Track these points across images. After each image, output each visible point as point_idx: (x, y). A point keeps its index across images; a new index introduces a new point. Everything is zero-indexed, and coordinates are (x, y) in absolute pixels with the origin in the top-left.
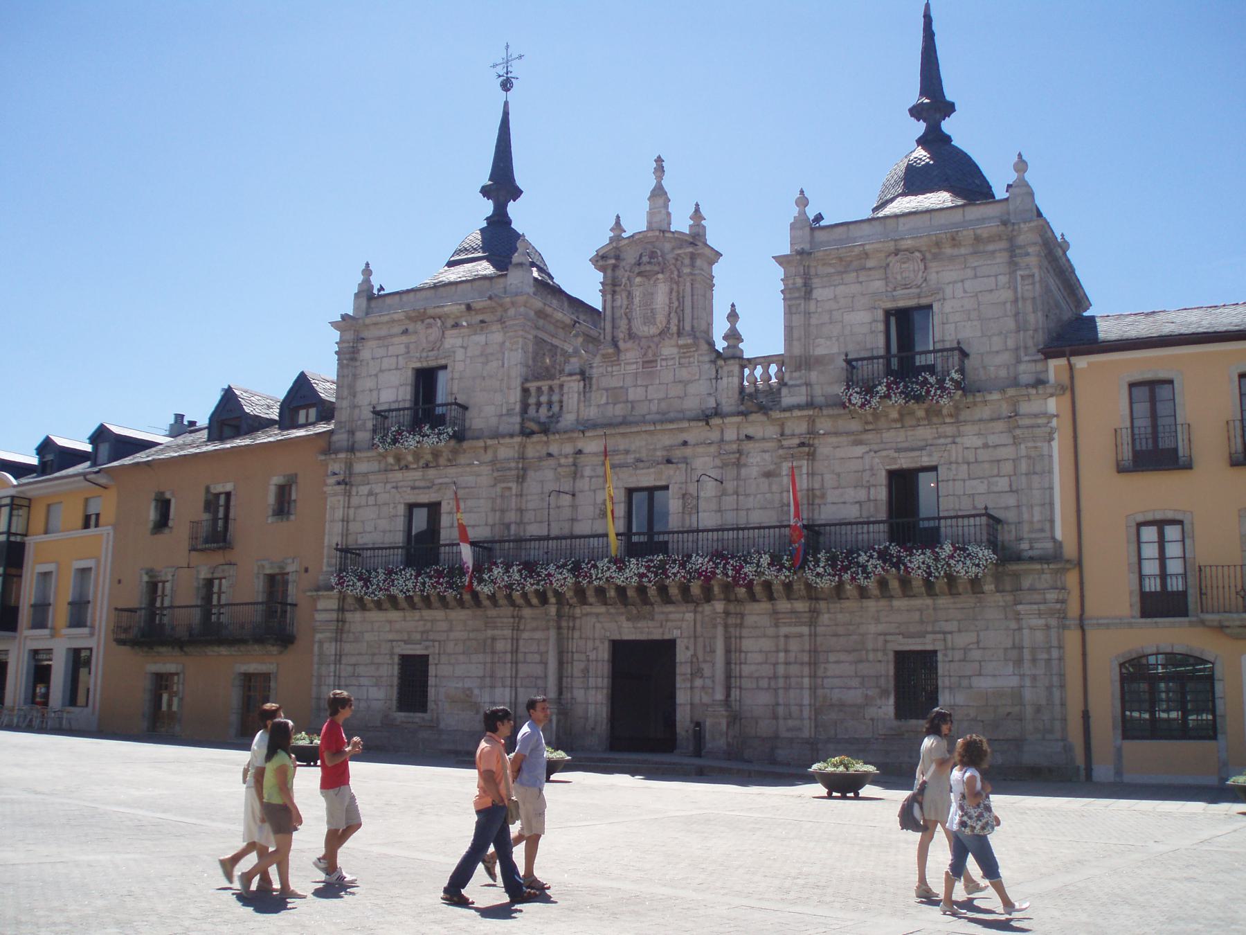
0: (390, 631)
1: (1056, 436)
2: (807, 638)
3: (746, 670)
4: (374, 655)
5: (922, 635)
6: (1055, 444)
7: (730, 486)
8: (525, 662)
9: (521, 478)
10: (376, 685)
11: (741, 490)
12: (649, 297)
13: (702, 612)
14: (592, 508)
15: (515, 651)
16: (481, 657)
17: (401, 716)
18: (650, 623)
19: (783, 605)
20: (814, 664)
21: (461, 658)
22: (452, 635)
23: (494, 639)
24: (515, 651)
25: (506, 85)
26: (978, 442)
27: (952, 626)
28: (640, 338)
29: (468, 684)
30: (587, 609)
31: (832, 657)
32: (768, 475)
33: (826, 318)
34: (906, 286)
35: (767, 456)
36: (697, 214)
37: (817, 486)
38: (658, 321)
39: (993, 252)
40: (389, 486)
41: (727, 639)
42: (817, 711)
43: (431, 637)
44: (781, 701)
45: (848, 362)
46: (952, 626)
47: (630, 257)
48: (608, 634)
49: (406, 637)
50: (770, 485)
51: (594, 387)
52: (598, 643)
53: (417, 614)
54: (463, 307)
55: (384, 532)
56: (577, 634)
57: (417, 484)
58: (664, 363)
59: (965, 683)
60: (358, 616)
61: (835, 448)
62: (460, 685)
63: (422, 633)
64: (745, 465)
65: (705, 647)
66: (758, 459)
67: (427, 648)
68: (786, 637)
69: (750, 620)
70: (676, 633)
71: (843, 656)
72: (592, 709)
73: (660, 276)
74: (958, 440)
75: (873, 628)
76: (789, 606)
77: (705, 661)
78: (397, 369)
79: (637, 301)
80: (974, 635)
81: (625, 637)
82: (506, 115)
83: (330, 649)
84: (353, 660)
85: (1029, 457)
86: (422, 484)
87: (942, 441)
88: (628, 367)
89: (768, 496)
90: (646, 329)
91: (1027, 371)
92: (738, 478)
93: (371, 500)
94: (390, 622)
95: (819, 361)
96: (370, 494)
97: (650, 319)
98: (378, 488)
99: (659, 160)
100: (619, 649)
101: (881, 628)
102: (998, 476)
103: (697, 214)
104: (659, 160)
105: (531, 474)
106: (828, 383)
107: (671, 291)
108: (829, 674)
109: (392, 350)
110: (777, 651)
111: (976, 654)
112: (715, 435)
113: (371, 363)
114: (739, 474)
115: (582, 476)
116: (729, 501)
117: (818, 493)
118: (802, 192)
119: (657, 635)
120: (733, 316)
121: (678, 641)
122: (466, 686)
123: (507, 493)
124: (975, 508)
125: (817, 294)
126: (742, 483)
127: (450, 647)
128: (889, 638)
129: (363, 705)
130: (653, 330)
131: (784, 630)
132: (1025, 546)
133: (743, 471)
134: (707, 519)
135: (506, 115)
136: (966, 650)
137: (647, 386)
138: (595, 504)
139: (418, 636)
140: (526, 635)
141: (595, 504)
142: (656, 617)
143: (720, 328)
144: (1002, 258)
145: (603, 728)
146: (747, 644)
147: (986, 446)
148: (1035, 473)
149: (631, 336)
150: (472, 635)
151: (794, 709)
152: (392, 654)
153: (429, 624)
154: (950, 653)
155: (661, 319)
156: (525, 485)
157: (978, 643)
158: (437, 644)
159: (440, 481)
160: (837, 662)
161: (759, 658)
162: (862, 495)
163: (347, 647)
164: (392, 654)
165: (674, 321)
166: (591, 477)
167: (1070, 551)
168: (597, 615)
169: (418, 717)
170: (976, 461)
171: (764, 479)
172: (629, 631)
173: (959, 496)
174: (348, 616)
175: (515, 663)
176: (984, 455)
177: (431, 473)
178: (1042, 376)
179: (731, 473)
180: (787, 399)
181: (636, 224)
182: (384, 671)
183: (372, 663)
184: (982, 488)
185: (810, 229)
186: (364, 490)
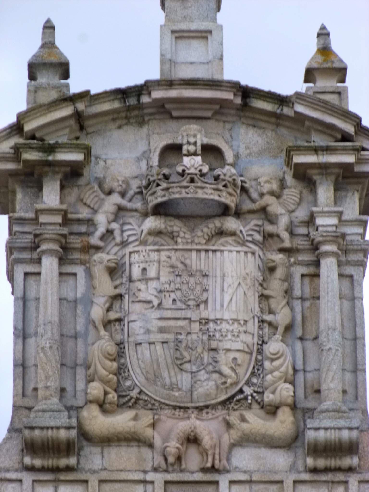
28: (152, 405)
36: (327, 67)
73: (231, 224)
79: (148, 292)
90: (185, 380)
103: (327, 67)
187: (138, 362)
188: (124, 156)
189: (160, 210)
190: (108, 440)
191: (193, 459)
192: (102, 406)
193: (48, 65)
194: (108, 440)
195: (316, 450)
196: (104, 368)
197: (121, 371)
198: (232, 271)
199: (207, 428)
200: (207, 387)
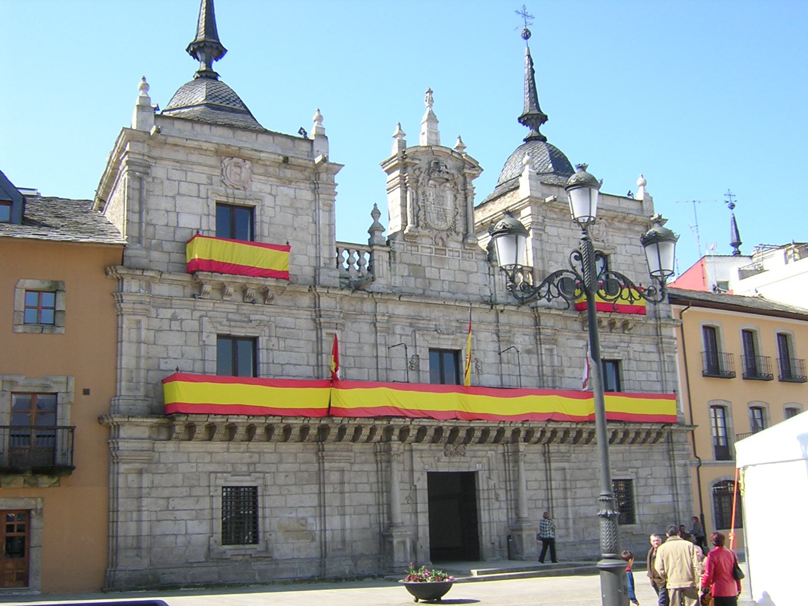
0: (211, 462)
4: (192, 487)
5: (626, 469)
10: (197, 518)
12: (440, 199)
18: (463, 459)
21: (293, 489)
22: (282, 467)
27: (638, 464)
28: (431, 229)
31: (579, 484)
32: (529, 352)
35: (527, 338)
40: (197, 314)
43: (258, 470)
48: (426, 467)
49: (230, 469)
50: (530, 360)
51: (398, 260)
54: (281, 158)
55: (194, 360)
57: (231, 316)
58: (451, 253)
59: (647, 499)
61: (568, 339)
63: (249, 464)
66: (521, 340)
70: (479, 467)
71: (584, 484)
74: (630, 345)
76: (556, 448)
77: (500, 488)
79: (431, 199)
80: (649, 469)
81: (440, 470)
84: (167, 493)
86: (237, 317)
88: (424, 250)
89: (530, 367)
93: (175, 325)
94: (211, 453)
96: (174, 318)
97: (442, 215)
98: (184, 314)
108: (578, 495)
111: (651, 482)
115: (394, 333)
121: (480, 473)
122: (300, 515)
127: (281, 479)
129: (181, 540)
130: (443, 226)
136: (646, 478)
137: (439, 269)
139: (245, 468)
142: (468, 454)
149: (427, 226)
150: (303, 467)
153: (257, 456)
155: (450, 217)
159: (257, 317)
160: (581, 488)
166: (401, 335)
167: (688, 422)
168: (421, 450)
169: (250, 548)
171: (526, 355)
172: (447, 465)
174: (159, 445)
177: (247, 308)
182: (205, 503)
183: (190, 496)
186: (167, 313)
199: (444, 235)
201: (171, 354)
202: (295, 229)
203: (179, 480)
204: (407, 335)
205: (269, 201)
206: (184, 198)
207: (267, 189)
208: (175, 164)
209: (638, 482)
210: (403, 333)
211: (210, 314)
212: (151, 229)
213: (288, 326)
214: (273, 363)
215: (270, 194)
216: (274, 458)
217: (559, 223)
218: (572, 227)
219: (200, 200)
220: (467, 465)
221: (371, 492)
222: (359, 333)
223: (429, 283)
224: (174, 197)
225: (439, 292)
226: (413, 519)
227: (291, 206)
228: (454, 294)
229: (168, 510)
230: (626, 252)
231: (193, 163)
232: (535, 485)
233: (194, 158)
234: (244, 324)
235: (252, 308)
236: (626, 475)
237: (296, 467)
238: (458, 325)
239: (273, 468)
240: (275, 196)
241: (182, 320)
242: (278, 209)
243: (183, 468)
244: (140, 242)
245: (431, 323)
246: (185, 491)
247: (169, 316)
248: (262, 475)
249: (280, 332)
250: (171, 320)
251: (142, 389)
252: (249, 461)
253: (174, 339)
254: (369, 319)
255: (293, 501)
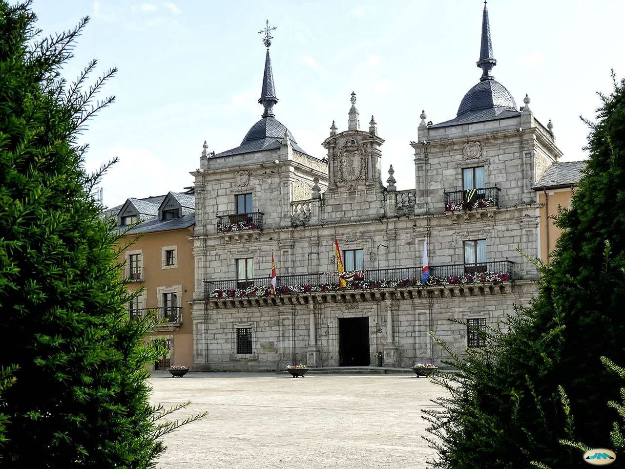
1: (539, 225)
2: (428, 315)
3: (401, 329)
4: (224, 329)
6: (538, 229)
7: (392, 249)
8: (298, 329)
9: (292, 247)
10: (226, 342)
11: (397, 251)
12: (351, 162)
13: (380, 305)
14: (327, 259)
15: (294, 325)
16: (277, 328)
17: (240, 356)
18: (357, 310)
19: (417, 301)
20: (431, 326)
21: (268, 329)
22: (262, 319)
23: (283, 319)
24: (294, 325)
25: (268, 44)
26: (504, 228)
27: (493, 308)
28: (347, 181)
29: (271, 340)
30: (327, 305)
31: (439, 322)
32: (409, 244)
33: (435, 172)
34: (472, 158)
36: (372, 122)
37: (431, 249)
38: (356, 173)
39: (513, 143)
41: (393, 315)
42: (433, 345)
44: (417, 342)
45: (446, 194)
46: (493, 308)
47: (341, 142)
48: (337, 315)
49: (240, 320)
52: (332, 320)
53: (245, 310)
55: (225, 272)
56: (322, 316)
57: (241, 250)
60: (215, 312)
62: (268, 341)
63: (248, 318)
64: (398, 240)
65: (382, 320)
67: (250, 325)
68: (419, 314)
69: (402, 307)
70: (369, 314)
71: (444, 322)
72: (331, 348)
73: (356, 152)
75: (457, 310)
78: (226, 195)
79: (345, 164)
81: (345, 317)
82: (268, 61)
83: (202, 327)
84: (214, 332)
85: (527, 235)
86: (243, 250)
87: (488, 228)
90: (350, 177)
91: (526, 198)
92: (395, 245)
93: (217, 258)
94: (231, 314)
95: (432, 192)
97: (351, 172)
98: (220, 252)
99: (353, 94)
100: (343, 322)
101: (461, 310)
102: (513, 243)
103: (372, 122)
104: (353, 94)
105: (297, 244)
106: (436, 203)
107: (362, 159)
108: (438, 329)
109: (223, 186)
110: (415, 321)
112: (384, 227)
113: (212, 192)
114: (395, 243)
115: (322, 245)
116: (391, 256)
117: (431, 251)
118: (423, 111)
119: (360, 315)
120: (391, 171)
122: (271, 341)
123: (286, 254)
124: (502, 257)
125: (430, 161)
126: (397, 247)
127: (262, 324)
128: (464, 313)
131: (417, 312)
132: (524, 273)
133: (398, 242)
134: (383, 264)
135: (268, 61)
137: (351, 204)
138: (329, 258)
139: (246, 320)
140: (298, 317)
141: (329, 258)
143: (385, 177)
144: (517, 145)
145: (336, 356)
146: (401, 318)
147: (508, 230)
148: (529, 242)
149: (343, 180)
151: (423, 345)
152: (233, 328)
154: (491, 319)
155: (357, 172)
156: (294, 249)
157: (504, 314)
158: (255, 323)
161: (407, 324)
162: (452, 252)
163: (210, 326)
164: (233, 328)
165: (363, 173)
166: (326, 246)
169: (248, 356)
170: (503, 237)
171: (407, 246)
173: (495, 252)
175: (294, 330)
176: (507, 234)
177: (247, 245)
178: (534, 199)
179: (392, 243)
180: (417, 211)
181: (343, 127)
184: (506, 248)
185: (427, 129)
186: (214, 253)
187: (345, 174)
188: (341, 142)
189: (346, 151)
190: (341, 187)
191: (352, 189)
192: (339, 182)
193: (333, 127)
194: (341, 187)
195: (367, 186)
196: (339, 176)
197: (342, 177)
198: (357, 160)
200: (353, 178)
201: (216, 271)
202: (271, 200)
203: (218, 326)
204: (330, 245)
205: (258, 188)
206: (220, 197)
207: (257, 182)
208: (214, 182)
209: (489, 320)
210: (327, 244)
211: (232, 250)
212: (207, 215)
213: (267, 250)
214: (260, 269)
215: (259, 185)
216: (258, 314)
217: (440, 154)
218: (451, 155)
219: (227, 196)
220: (362, 313)
221: (306, 329)
222: (303, 248)
223: (345, 213)
224: (216, 198)
225: (350, 217)
226: (332, 344)
227: (270, 188)
228: (360, 217)
229: (214, 339)
230: (499, 160)
231: (222, 179)
232: (407, 324)
233: (224, 176)
234: (246, 253)
235: (250, 244)
236: (480, 316)
237: (268, 318)
238: (361, 234)
239: (258, 319)
240: (261, 185)
241: (220, 255)
242: (262, 191)
243: (220, 321)
244: (201, 223)
245: (344, 236)
246: (221, 331)
247: (215, 254)
248: (252, 323)
249: (263, 253)
250: (216, 255)
251: (203, 288)
252: (248, 316)
253: (216, 264)
254: (308, 240)
255: (267, 334)
